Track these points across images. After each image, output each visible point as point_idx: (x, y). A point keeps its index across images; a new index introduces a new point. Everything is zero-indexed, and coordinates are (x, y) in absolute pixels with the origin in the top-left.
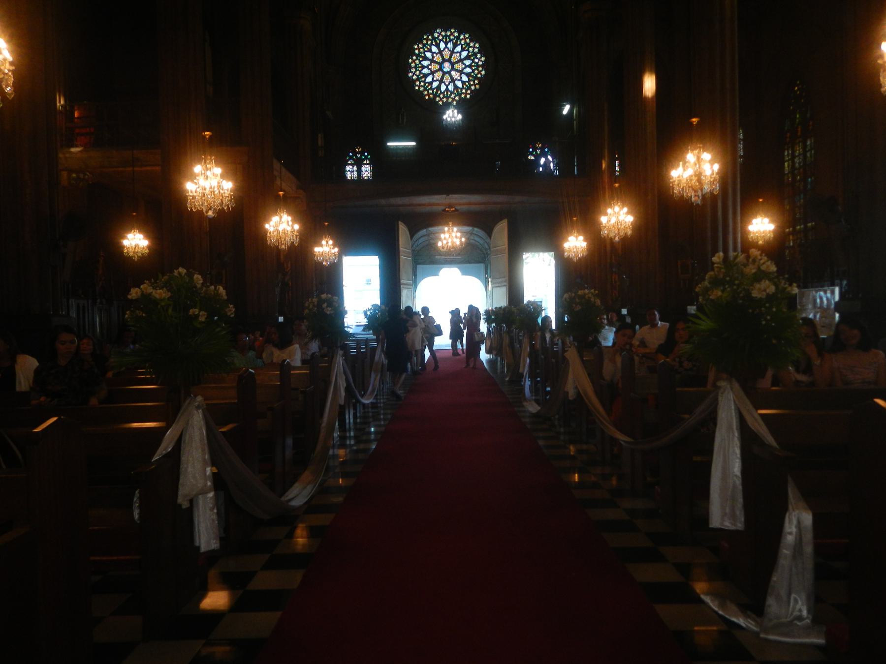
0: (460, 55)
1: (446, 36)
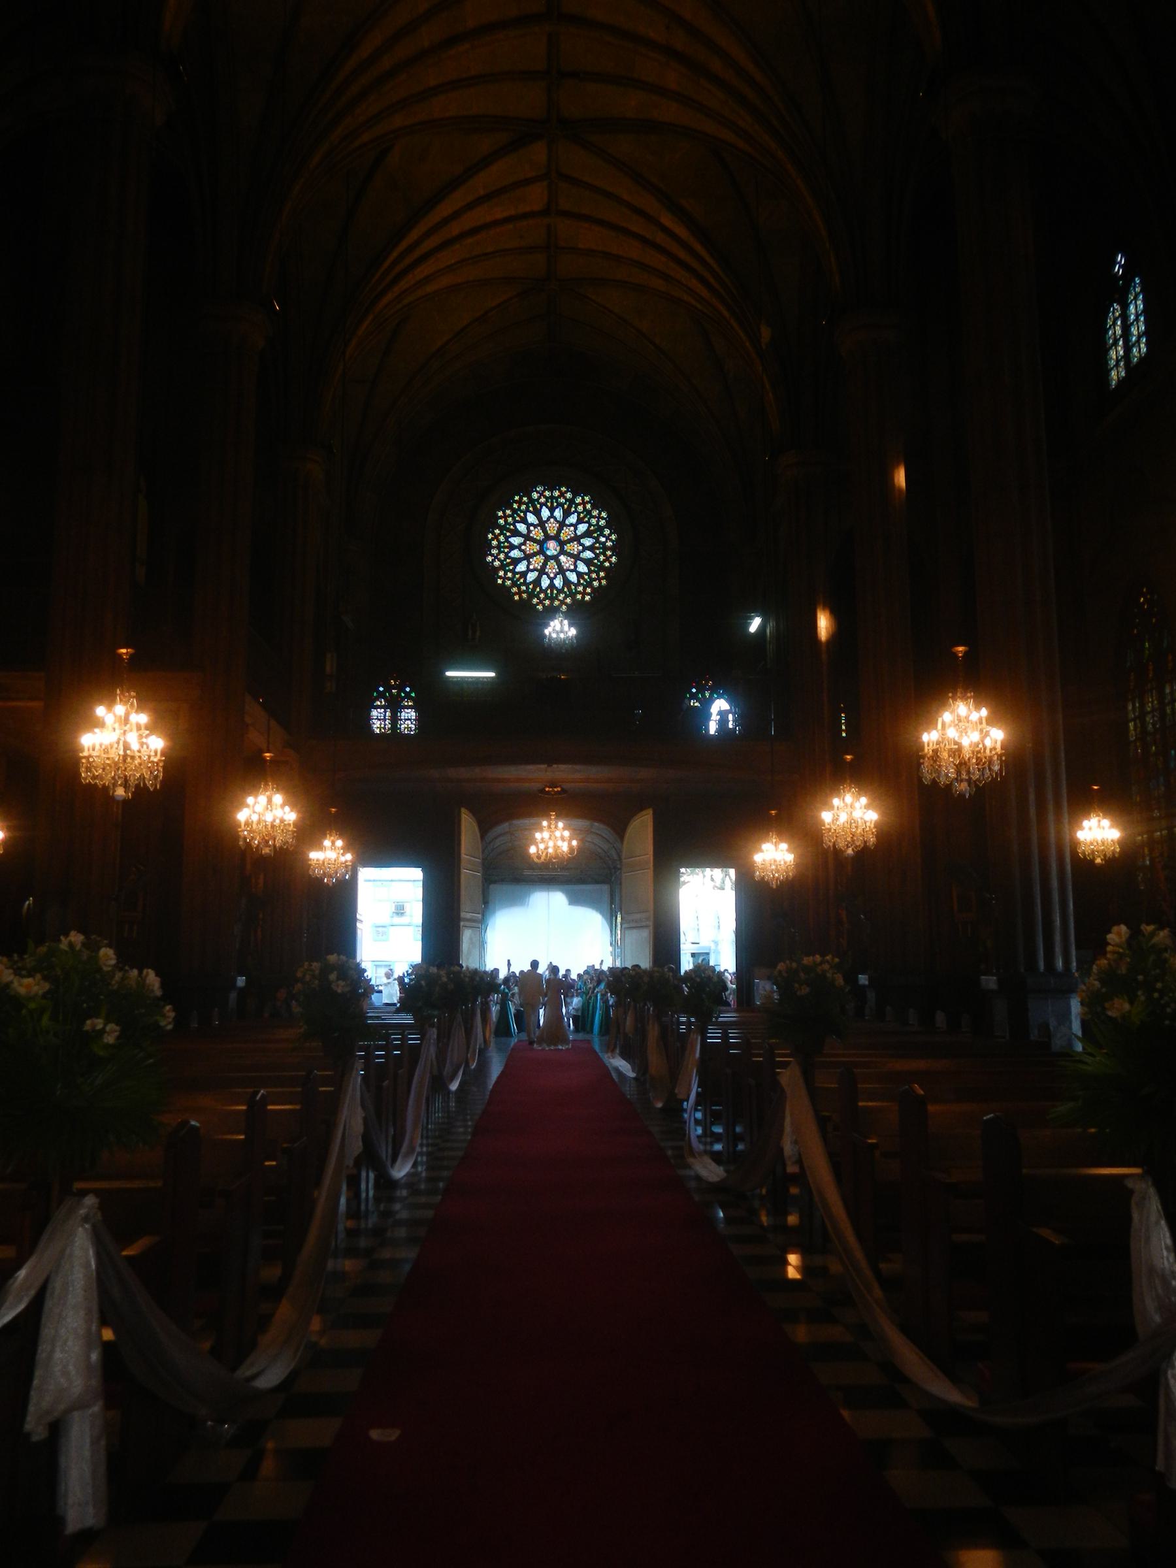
0: (576, 529)
1: (552, 497)
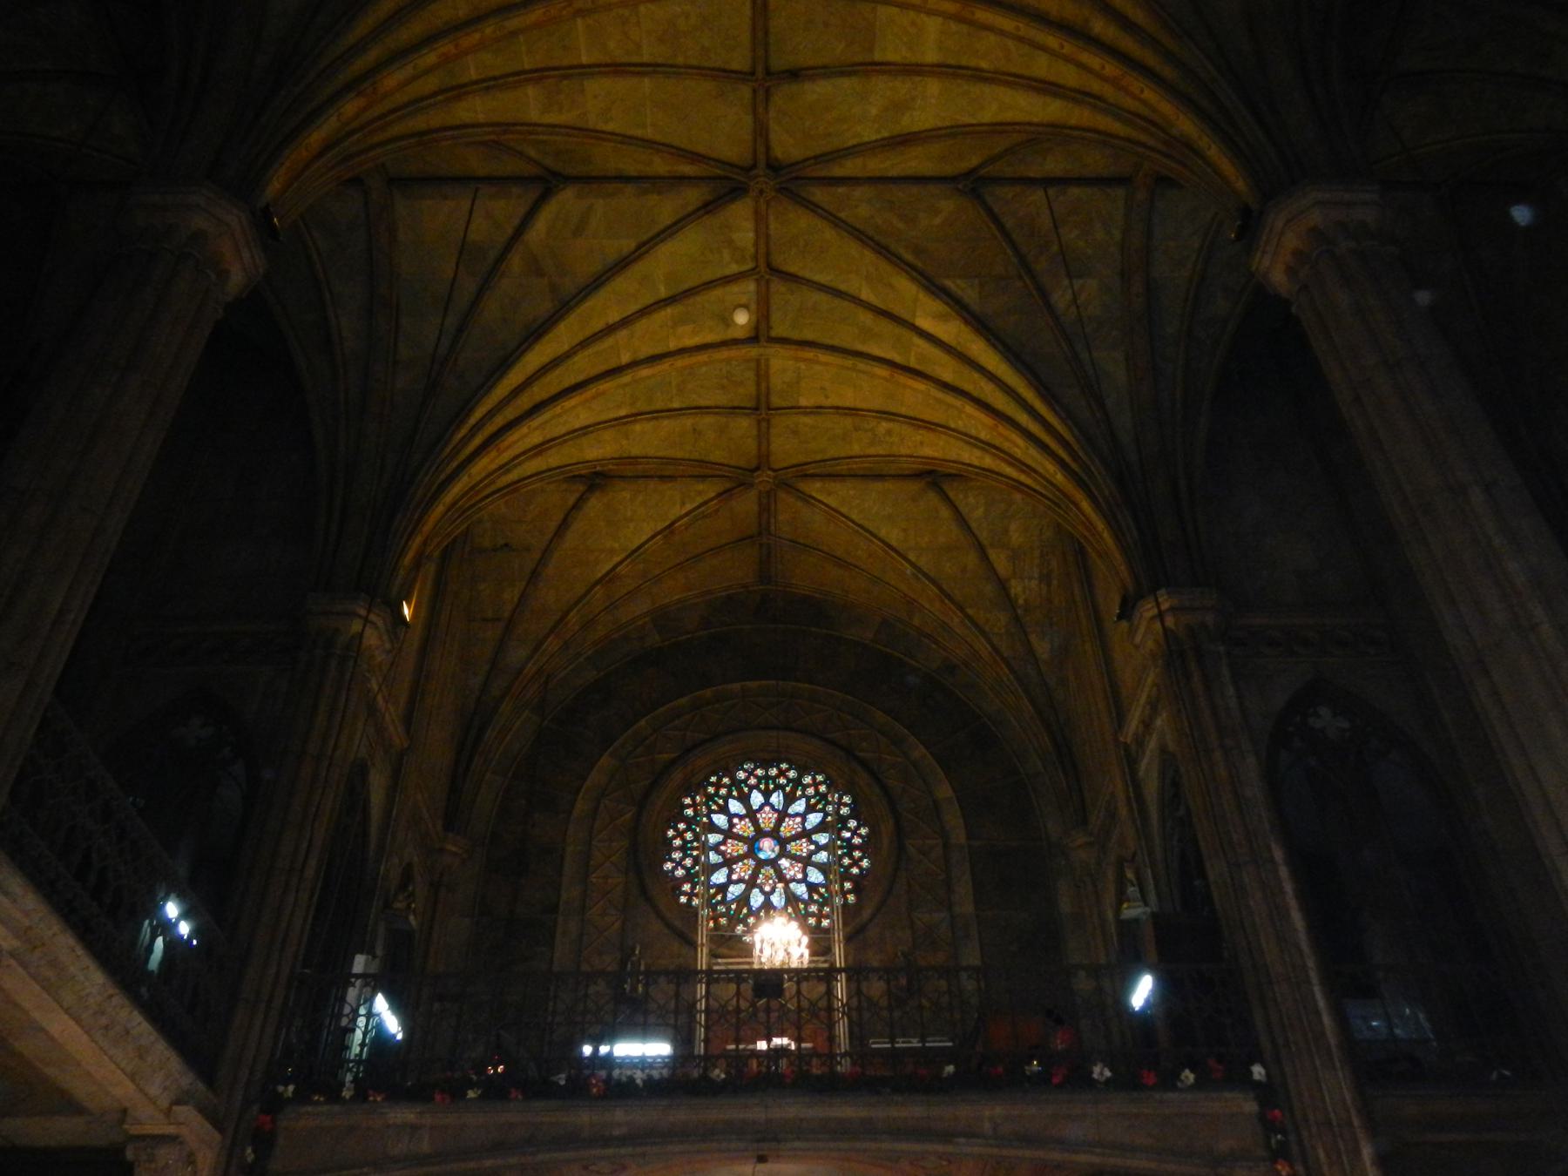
0: (804, 820)
1: (767, 778)
